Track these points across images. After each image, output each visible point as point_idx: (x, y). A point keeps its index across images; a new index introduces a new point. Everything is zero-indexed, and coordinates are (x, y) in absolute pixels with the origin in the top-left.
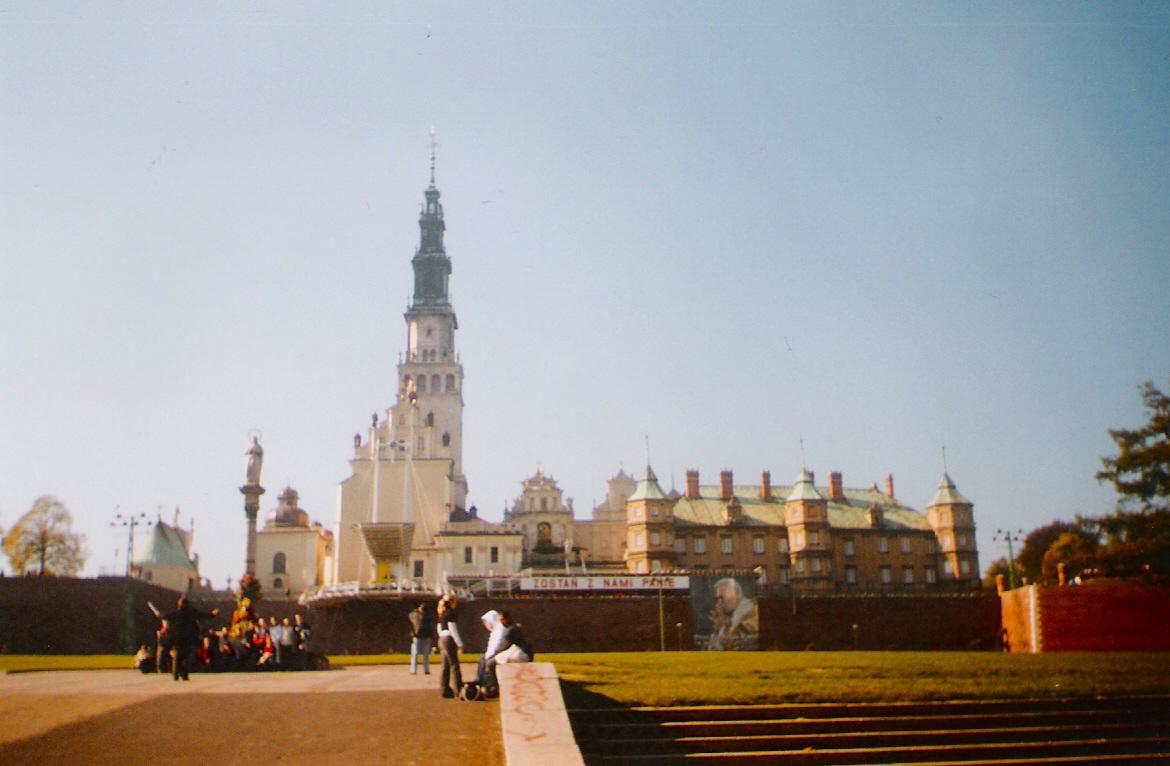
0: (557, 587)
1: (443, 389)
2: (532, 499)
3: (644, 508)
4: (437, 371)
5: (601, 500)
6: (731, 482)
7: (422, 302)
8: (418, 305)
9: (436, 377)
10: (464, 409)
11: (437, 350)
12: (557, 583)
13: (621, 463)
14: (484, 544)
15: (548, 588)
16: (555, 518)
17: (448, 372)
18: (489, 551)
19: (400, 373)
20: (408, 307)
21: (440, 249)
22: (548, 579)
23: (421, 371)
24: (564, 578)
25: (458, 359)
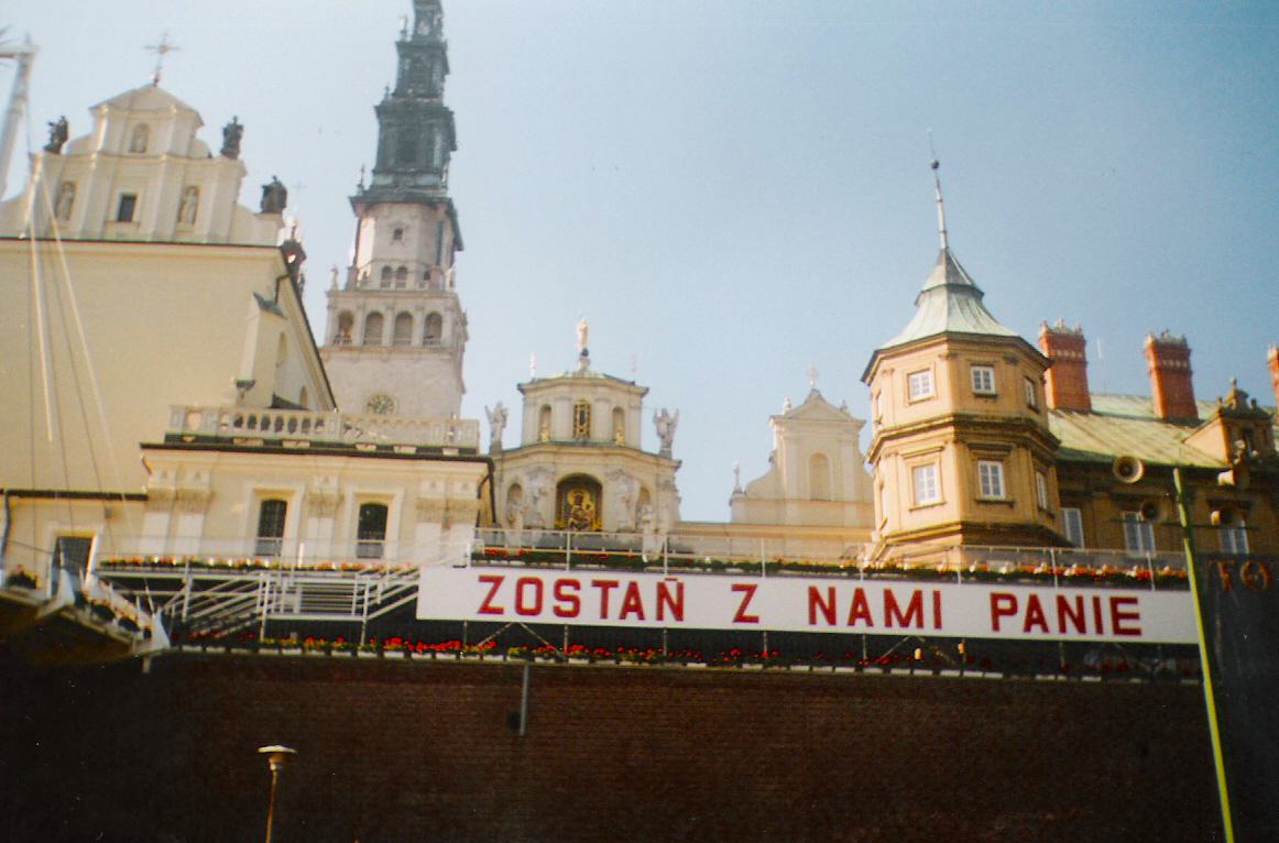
0: (589, 616)
1: (417, 340)
2: (547, 409)
3: (943, 368)
4: (406, 305)
5: (755, 470)
6: (1185, 374)
7: (388, 180)
8: (386, 187)
9: (404, 317)
10: (464, 397)
11: (411, 267)
12: (590, 598)
13: (814, 374)
14: (331, 489)
15: (547, 617)
16: (617, 462)
17: (429, 310)
18: (350, 519)
19: (329, 307)
20: (360, 186)
21: (434, 93)
22: (549, 577)
23: (374, 305)
24: (624, 579)
25: (452, 284)
